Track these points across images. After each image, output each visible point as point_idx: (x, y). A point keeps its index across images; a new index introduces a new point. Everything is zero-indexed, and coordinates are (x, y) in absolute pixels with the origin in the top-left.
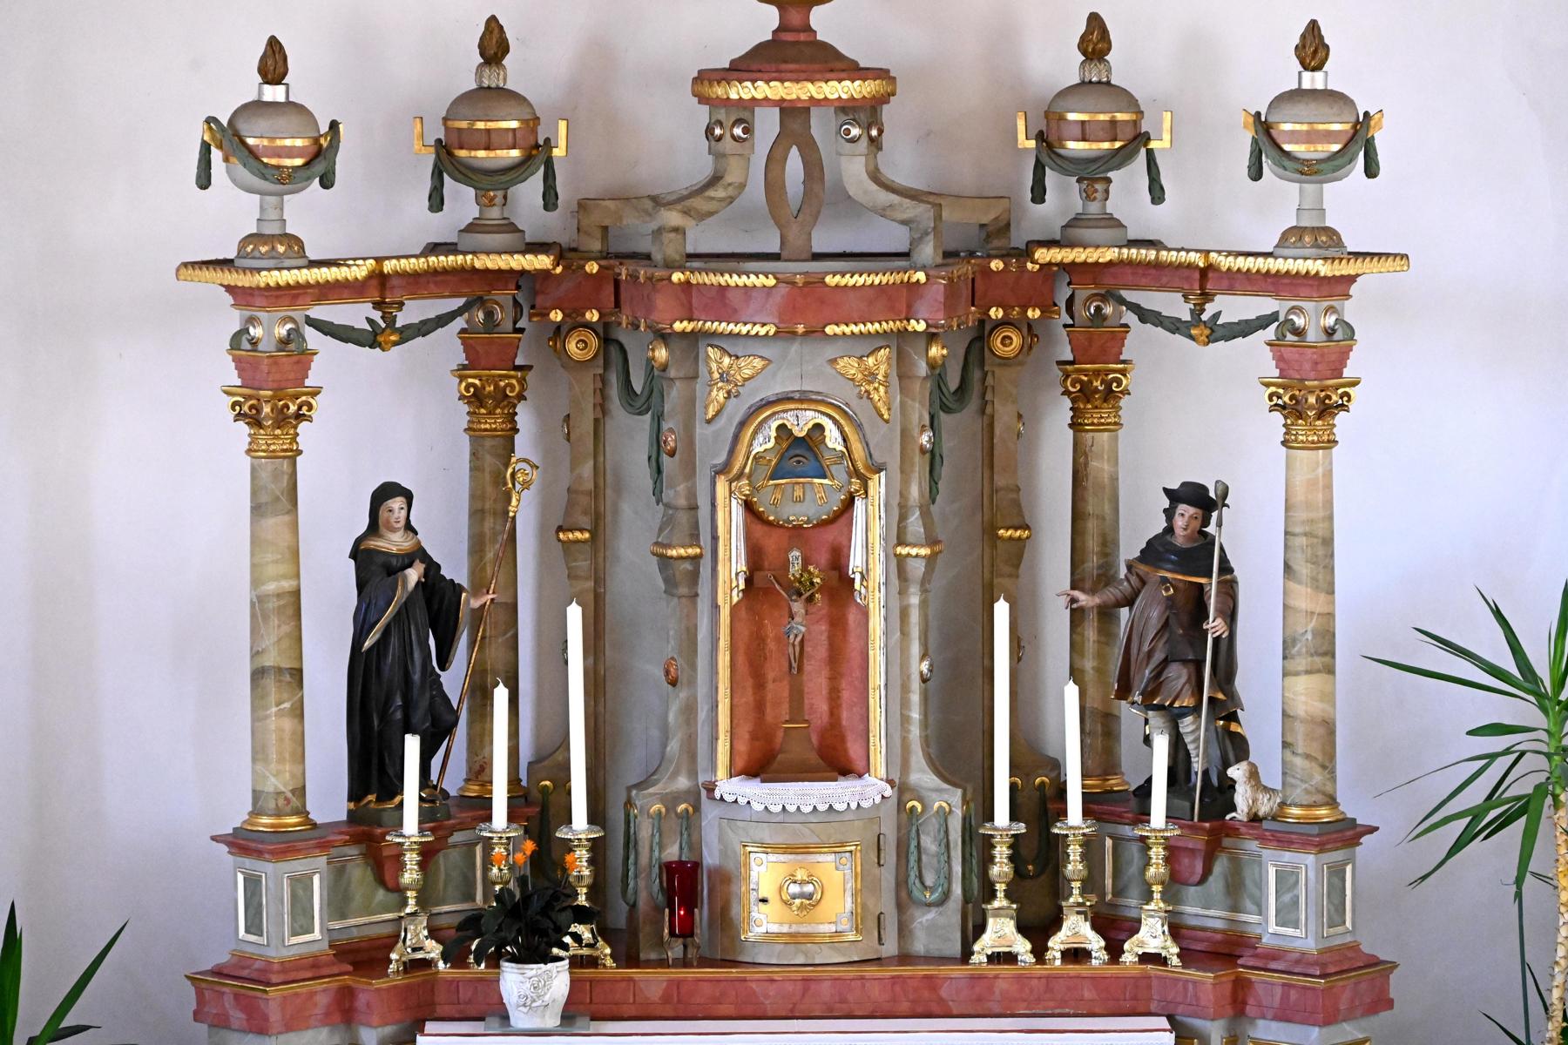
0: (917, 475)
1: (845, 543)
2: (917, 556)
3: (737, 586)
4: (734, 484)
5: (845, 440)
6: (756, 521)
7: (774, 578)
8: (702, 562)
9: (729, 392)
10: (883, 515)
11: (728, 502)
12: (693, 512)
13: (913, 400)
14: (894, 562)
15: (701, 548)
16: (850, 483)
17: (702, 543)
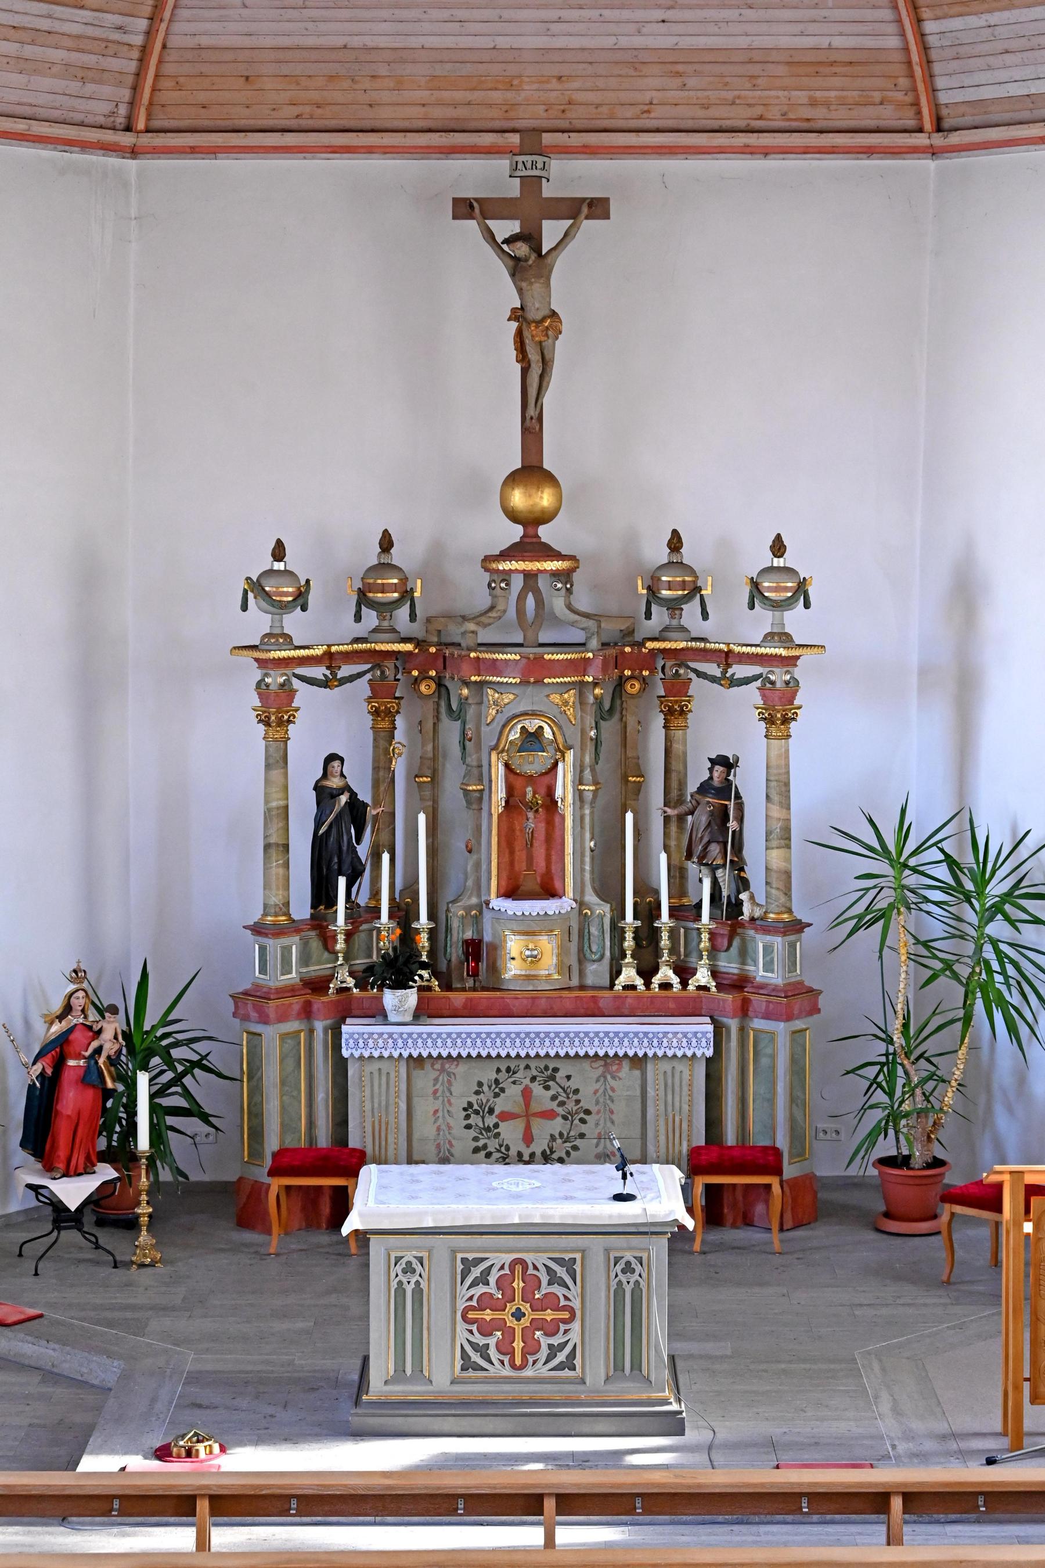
9: (497, 711)
14: (577, 793)
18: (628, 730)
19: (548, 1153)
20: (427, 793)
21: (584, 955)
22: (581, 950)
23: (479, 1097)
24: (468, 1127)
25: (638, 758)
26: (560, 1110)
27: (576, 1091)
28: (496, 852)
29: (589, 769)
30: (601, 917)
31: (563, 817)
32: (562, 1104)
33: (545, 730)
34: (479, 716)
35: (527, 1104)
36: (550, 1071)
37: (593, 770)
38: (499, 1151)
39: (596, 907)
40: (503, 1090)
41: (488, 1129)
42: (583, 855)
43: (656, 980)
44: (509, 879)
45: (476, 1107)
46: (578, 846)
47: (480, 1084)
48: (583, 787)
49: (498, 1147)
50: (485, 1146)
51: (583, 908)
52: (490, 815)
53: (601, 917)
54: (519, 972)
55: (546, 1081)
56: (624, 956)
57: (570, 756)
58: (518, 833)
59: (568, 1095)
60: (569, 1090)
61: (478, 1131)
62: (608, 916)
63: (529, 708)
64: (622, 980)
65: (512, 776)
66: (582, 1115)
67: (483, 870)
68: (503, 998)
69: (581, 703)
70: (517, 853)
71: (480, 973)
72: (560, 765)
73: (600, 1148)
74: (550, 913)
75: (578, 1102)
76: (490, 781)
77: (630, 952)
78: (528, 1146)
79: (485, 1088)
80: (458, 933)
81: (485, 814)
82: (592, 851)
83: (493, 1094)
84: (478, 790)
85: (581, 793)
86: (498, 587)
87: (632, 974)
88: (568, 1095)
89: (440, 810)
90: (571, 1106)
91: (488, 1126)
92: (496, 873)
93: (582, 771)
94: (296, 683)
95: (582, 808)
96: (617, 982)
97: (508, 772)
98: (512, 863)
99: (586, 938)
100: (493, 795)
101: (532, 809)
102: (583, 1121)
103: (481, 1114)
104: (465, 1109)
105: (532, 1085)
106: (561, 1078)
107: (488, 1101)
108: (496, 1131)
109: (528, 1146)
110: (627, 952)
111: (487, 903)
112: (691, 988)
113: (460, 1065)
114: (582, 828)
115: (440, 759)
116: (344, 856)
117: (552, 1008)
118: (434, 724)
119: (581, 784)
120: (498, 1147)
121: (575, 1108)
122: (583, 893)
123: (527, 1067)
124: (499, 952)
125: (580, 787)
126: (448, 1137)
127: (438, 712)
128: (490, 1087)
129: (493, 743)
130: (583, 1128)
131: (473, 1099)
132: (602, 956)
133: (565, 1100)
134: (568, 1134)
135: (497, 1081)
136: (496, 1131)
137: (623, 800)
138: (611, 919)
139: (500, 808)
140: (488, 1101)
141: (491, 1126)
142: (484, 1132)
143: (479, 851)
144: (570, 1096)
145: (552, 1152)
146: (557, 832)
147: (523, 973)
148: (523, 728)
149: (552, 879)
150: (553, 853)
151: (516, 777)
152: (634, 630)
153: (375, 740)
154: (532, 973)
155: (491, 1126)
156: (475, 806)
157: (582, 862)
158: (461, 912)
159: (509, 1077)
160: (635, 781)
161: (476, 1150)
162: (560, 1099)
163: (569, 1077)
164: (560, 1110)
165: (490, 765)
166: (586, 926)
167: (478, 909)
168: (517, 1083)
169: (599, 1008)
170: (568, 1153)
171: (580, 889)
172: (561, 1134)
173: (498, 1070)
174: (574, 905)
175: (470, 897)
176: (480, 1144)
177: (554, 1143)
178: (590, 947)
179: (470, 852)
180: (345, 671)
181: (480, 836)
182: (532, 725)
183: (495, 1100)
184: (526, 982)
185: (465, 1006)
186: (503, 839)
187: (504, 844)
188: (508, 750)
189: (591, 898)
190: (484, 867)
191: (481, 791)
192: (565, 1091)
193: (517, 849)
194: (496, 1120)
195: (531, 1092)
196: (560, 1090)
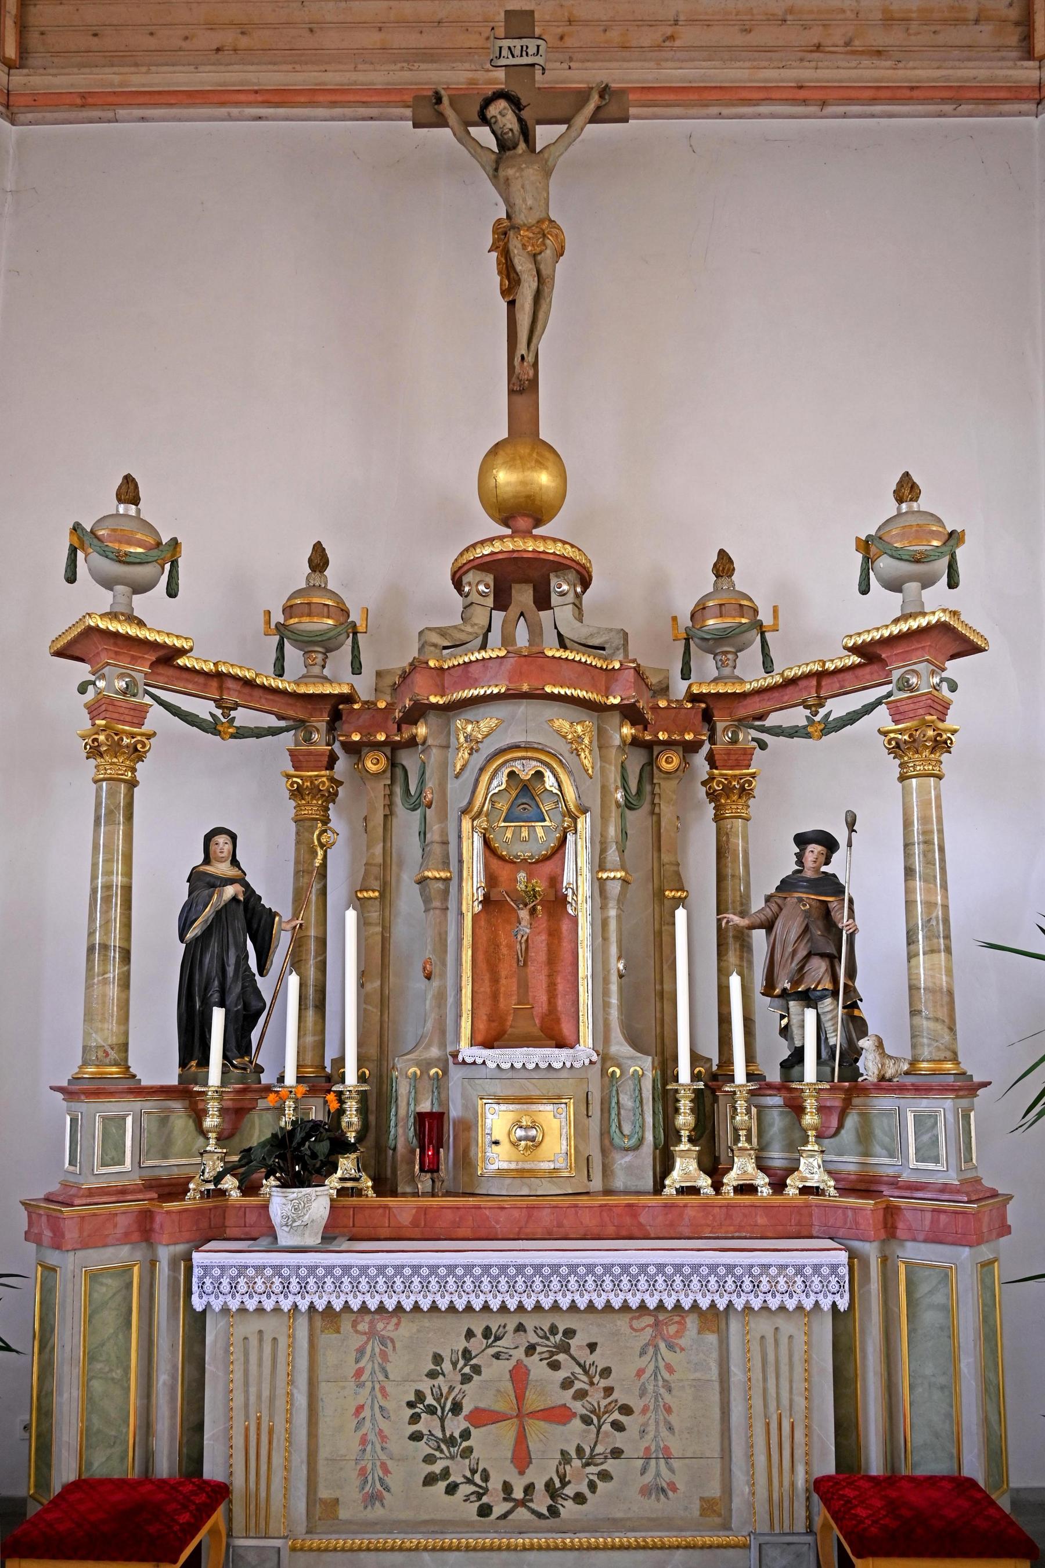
1: (559, 871)
2: (614, 878)
4: (475, 823)
8: (452, 883)
9: (472, 749)
10: (589, 845)
12: (444, 846)
14: (597, 884)
16: (564, 821)
18: (663, 824)
19: (558, 1485)
20: (374, 915)
21: (611, 1140)
22: (605, 1133)
23: (436, 1382)
24: (416, 1437)
25: (678, 865)
26: (578, 1407)
27: (606, 1372)
28: (470, 974)
29: (614, 847)
30: (638, 1078)
31: (575, 920)
32: (581, 1395)
33: (546, 779)
34: (444, 765)
35: (520, 1397)
36: (560, 1334)
37: (622, 851)
38: (470, 1481)
39: (629, 1062)
40: (477, 1370)
41: (451, 1441)
42: (606, 981)
43: (731, 1179)
44: (491, 1019)
45: (430, 1400)
47: (438, 1359)
49: (468, 1474)
50: (446, 1473)
51: (609, 1063)
52: (461, 914)
53: (638, 1078)
54: (504, 1165)
55: (552, 1354)
56: (679, 1140)
57: (584, 823)
58: (504, 950)
59: (591, 1378)
60: (592, 1370)
61: (433, 1444)
62: (649, 1075)
63: (519, 738)
64: (676, 1178)
65: (495, 863)
66: (616, 1416)
68: (479, 1208)
69: (600, 748)
70: (503, 981)
71: (442, 1167)
72: (570, 838)
73: (649, 1477)
74: (557, 1065)
75: (609, 1391)
76: (461, 862)
77: (687, 1133)
78: (522, 1473)
79: (447, 1366)
81: (452, 915)
82: (621, 976)
83: (459, 1378)
84: (441, 879)
85: (602, 882)
86: (474, 589)
87: (691, 1168)
88: (591, 1378)
90: (596, 1397)
91: (452, 1436)
92: (470, 1007)
93: (603, 851)
94: (157, 718)
95: (604, 907)
96: (667, 1182)
97: (488, 853)
98: (495, 996)
99: (614, 1113)
100: (464, 884)
101: (526, 905)
102: (617, 1426)
103: (439, 1412)
104: (411, 1405)
105: (527, 1361)
106: (580, 1347)
107: (451, 1389)
108: (465, 1444)
109: (522, 1473)
110: (683, 1133)
111: (455, 1056)
112: (791, 1191)
113: (403, 1324)
114: (605, 939)
115: (394, 867)
116: (229, 980)
117: (560, 1225)
118: (385, 816)
119: (602, 868)
120: (468, 1474)
121: (604, 1403)
122: (607, 1040)
123: (520, 1328)
124: (473, 1134)
125: (600, 875)
126: (383, 1457)
127: (391, 795)
128: (454, 1364)
130: (619, 1440)
131: (425, 1386)
132: (641, 1141)
133: (587, 1387)
134: (592, 1450)
135: (467, 1354)
136: (465, 1444)
137: (657, 926)
138: (654, 1081)
139: (476, 903)
140: (451, 1389)
141: (457, 1435)
142: (443, 1446)
143: (443, 975)
144: (596, 1380)
145: (564, 1484)
146: (566, 945)
147: (513, 1166)
148: (512, 775)
149: (558, 1021)
150: (559, 980)
151: (500, 862)
152: (667, 688)
153: (298, 833)
154: (527, 1166)
155: (457, 1435)
156: (436, 904)
157: (606, 993)
158: (412, 1070)
159: (488, 1347)
160: (674, 898)
161: (430, 1480)
162: (578, 1385)
163: (592, 1347)
164: (578, 1407)
165: (460, 837)
166: (614, 1093)
167: (441, 1065)
168: (503, 1356)
169: (640, 1224)
170: (592, 1487)
171: (603, 1036)
172: (579, 1450)
173: (470, 1334)
174: (595, 1058)
175: (429, 1046)
176: (437, 1468)
177: (568, 1467)
178: (620, 1127)
179: (428, 977)
180: (243, 717)
181: (446, 952)
182: (526, 770)
183: (465, 1387)
184: (518, 1181)
185: (415, 1224)
186: (481, 956)
187: (482, 965)
188: (487, 815)
189: (620, 1047)
190: (450, 1000)
191: (447, 880)
192: (586, 1372)
193: (503, 973)
194: (465, 1425)
195: (527, 1372)
196: (578, 1370)
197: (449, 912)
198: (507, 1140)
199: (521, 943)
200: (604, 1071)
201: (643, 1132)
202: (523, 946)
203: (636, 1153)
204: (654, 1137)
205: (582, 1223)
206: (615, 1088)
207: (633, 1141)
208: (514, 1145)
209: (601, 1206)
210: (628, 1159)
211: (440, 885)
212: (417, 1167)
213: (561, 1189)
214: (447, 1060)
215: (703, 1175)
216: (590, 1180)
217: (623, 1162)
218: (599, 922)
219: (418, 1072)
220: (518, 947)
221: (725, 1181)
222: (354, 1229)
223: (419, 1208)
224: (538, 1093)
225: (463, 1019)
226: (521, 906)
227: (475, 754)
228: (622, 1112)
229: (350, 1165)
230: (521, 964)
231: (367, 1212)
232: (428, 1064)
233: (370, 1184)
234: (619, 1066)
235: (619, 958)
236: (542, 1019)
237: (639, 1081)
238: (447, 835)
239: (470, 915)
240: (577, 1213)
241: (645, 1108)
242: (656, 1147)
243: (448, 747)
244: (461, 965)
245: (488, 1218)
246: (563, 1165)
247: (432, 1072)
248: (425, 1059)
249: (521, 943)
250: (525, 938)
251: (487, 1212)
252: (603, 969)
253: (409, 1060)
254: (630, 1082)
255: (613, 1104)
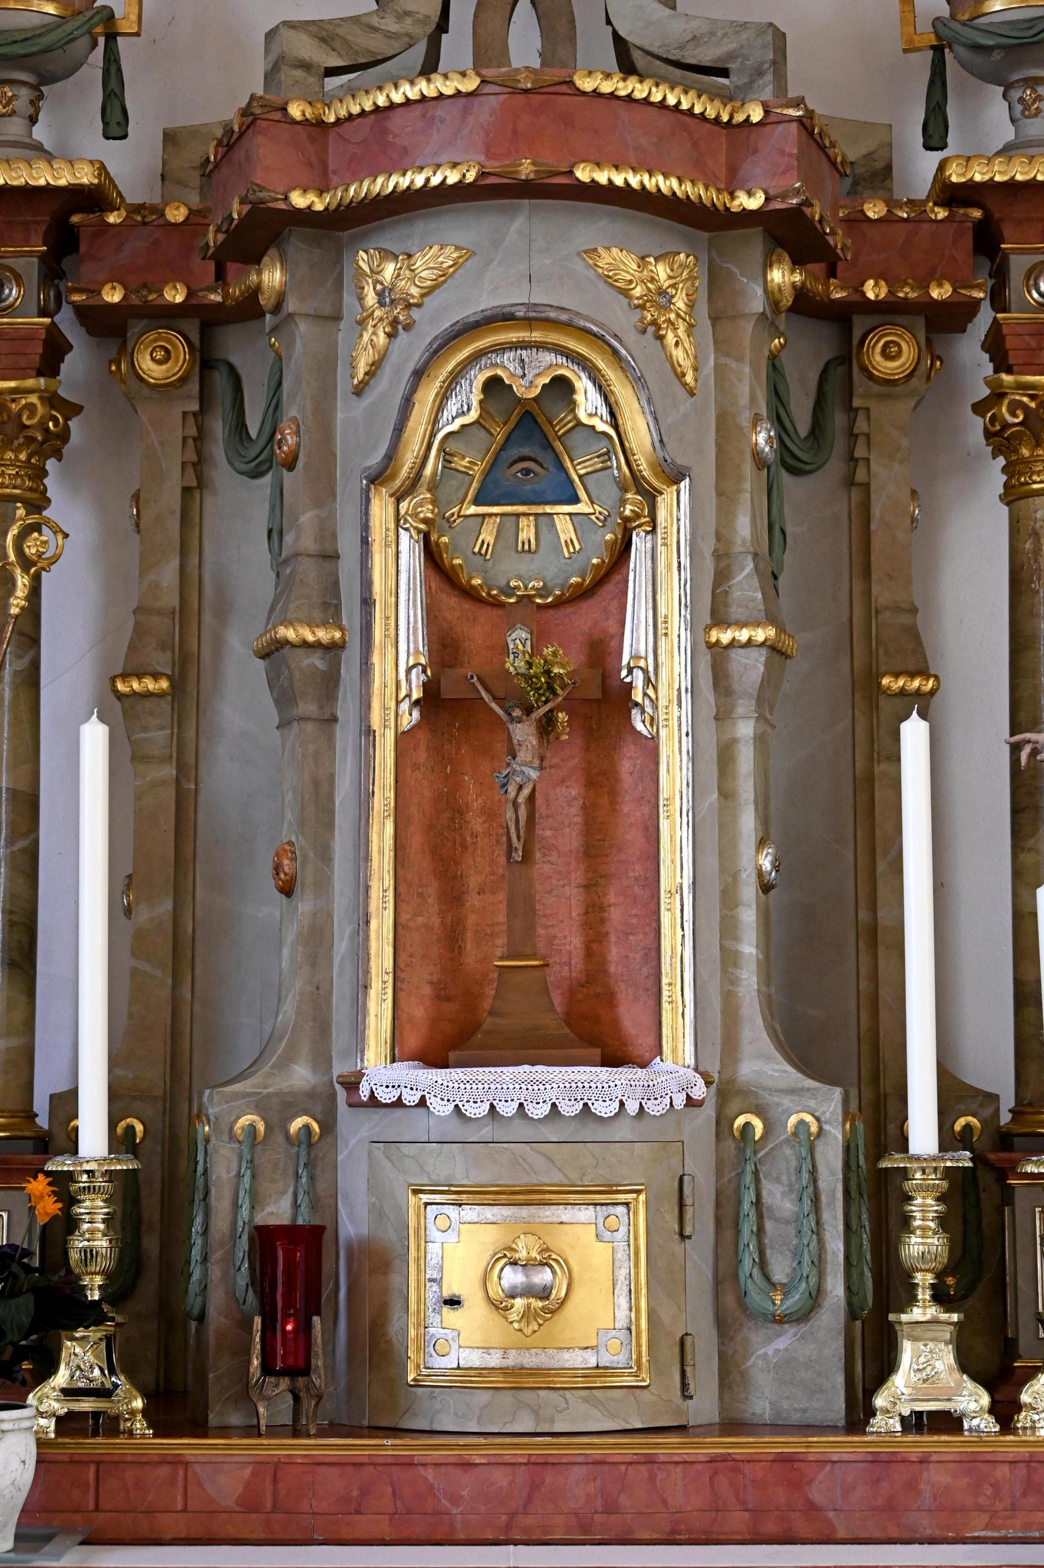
0: (748, 496)
1: (613, 630)
2: (749, 643)
3: (408, 696)
4: (404, 506)
5: (612, 414)
6: (446, 587)
7: (480, 679)
8: (344, 655)
9: (395, 322)
10: (685, 560)
11: (392, 534)
12: (327, 565)
13: (740, 359)
15: (342, 629)
16: (623, 502)
17: (344, 622)
20: (158, 737)
21: (742, 1296)
28: (389, 881)
29: (750, 566)
31: (651, 748)
33: (579, 397)
39: (787, 1102)
42: (729, 899)
44: (441, 994)
46: (711, 862)
48: (726, 637)
51: (734, 1105)
52: (369, 732)
54: (473, 1359)
58: (477, 823)
62: (836, 1134)
65: (452, 605)
67: (337, 960)
68: (409, 1464)
69: (715, 319)
70: (474, 900)
71: (318, 1362)
72: (640, 543)
74: (604, 1109)
76: (367, 602)
77: (930, 1279)
80: (236, 1206)
81: (345, 736)
82: (766, 888)
84: (318, 645)
87: (939, 1365)
89: (201, 798)
92: (389, 964)
93: (722, 576)
95: (723, 716)
96: (880, 1401)
99: (748, 1228)
100: (376, 659)
101: (529, 710)
110: (919, 1278)
111: (352, 1085)
114: (727, 795)
115: (208, 618)
117: (611, 1508)
118: (186, 491)
119: (719, 620)
122: (730, 1048)
124: (395, 1279)
125: (714, 636)
129: (376, 458)
132: (816, 1297)
138: (847, 1149)
139: (405, 706)
143: (323, 885)
146: (630, 809)
147: (494, 1360)
148: (494, 386)
149: (610, 999)
150: (612, 897)
151: (467, 605)
154: (530, 1360)
156: (307, 707)
157: (729, 928)
158: (245, 1120)
165: (365, 542)
166: (748, 1178)
167: (318, 1110)
169: (812, 1508)
174: (699, 1091)
178: (763, 1264)
179: (287, 890)
181: (330, 826)
184: (508, 1398)
185: (250, 1504)
186: (416, 839)
187: (420, 860)
190: (341, 946)
191: (334, 648)
193: (474, 881)
197: (338, 729)
198: (480, 1294)
199: (515, 805)
200: (722, 1123)
201: (821, 1275)
202: (523, 812)
203: (804, 1328)
204: (848, 1288)
205: (665, 1502)
206: (750, 1168)
207: (796, 1299)
208: (499, 1307)
209: (713, 1460)
210: (782, 1343)
211: (317, 661)
212: (256, 1362)
213: (613, 1416)
214: (333, 1097)
215: (969, 1384)
216: (686, 1396)
217: (770, 1350)
218: (711, 754)
219: (261, 1127)
220: (510, 814)
221: (1025, 1398)
222: (101, 1516)
223: (260, 1464)
224: (557, 1177)
225: (373, 993)
226: (517, 713)
227: (402, 335)
228: (769, 1225)
229: (90, 1357)
230: (518, 856)
231: (130, 1475)
232: (290, 1106)
233: (138, 1404)
234: (759, 1111)
235: (761, 843)
236: (571, 993)
237: (812, 1150)
238: (334, 536)
239: (390, 735)
240: (652, 1478)
241: (826, 1216)
242: (852, 1314)
243: (337, 318)
244: (368, 858)
245: (432, 1487)
246: (621, 1359)
247: (296, 1124)
248: (277, 1094)
249: (515, 805)
250: (526, 792)
251: (430, 1474)
252: (722, 870)
253: (237, 1096)
254: (788, 1151)
255: (746, 1206)
